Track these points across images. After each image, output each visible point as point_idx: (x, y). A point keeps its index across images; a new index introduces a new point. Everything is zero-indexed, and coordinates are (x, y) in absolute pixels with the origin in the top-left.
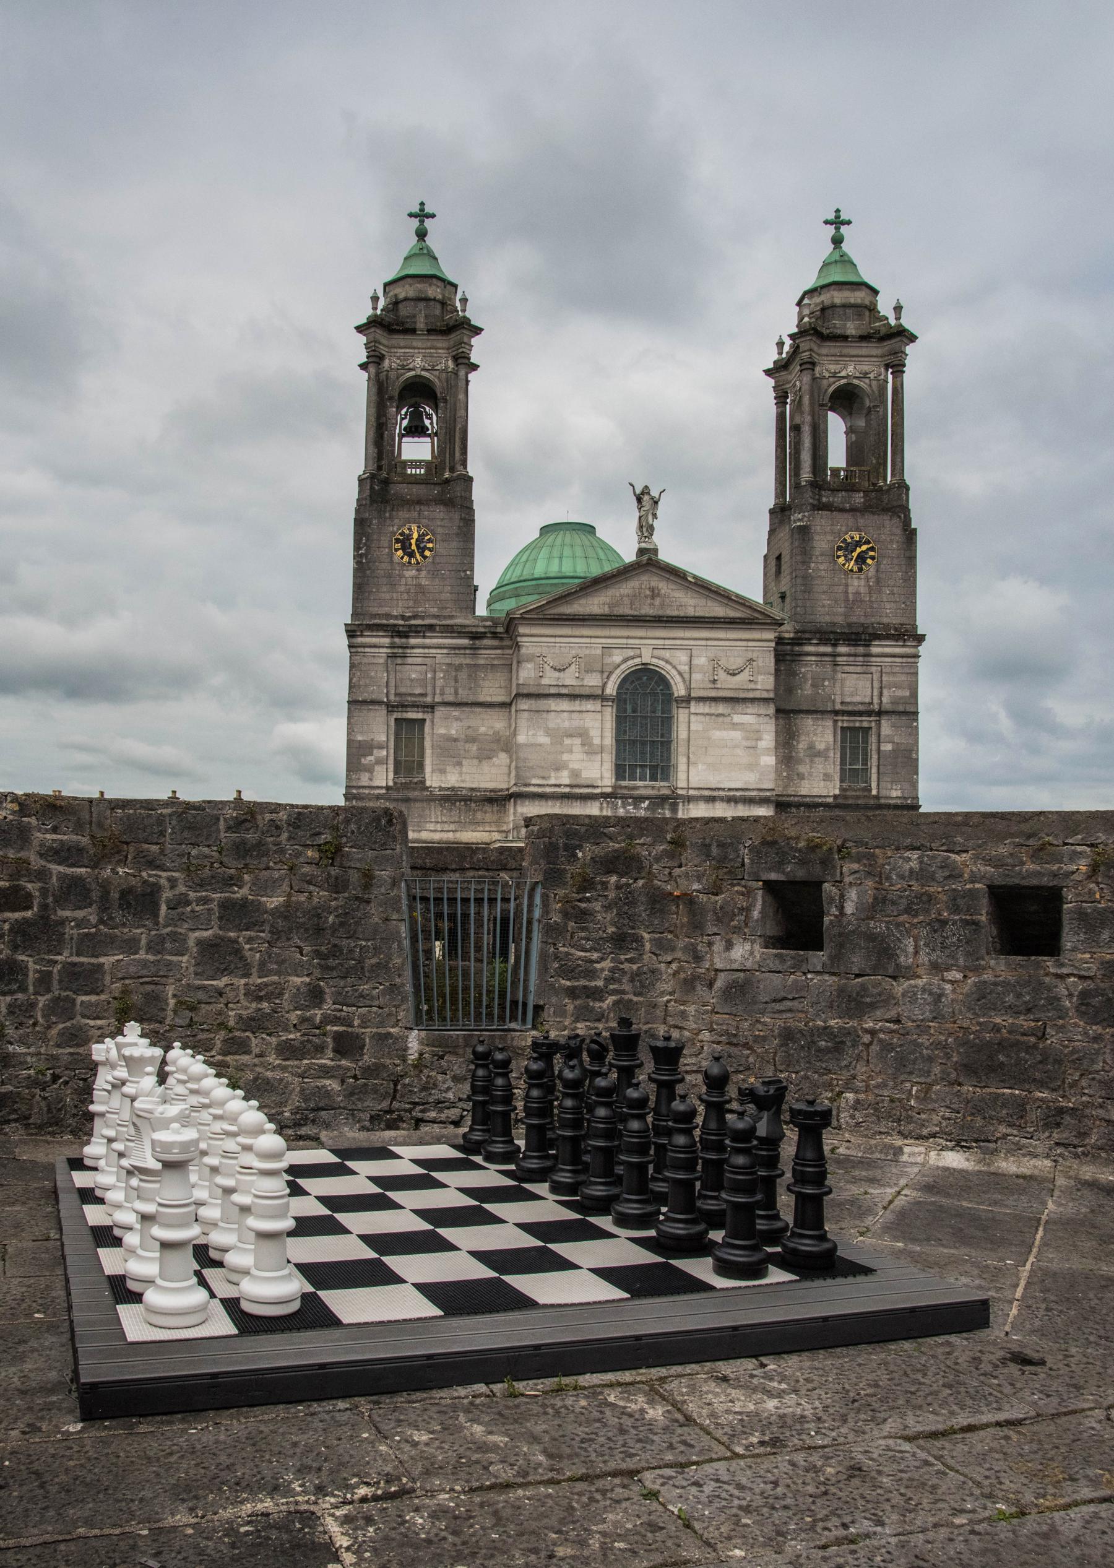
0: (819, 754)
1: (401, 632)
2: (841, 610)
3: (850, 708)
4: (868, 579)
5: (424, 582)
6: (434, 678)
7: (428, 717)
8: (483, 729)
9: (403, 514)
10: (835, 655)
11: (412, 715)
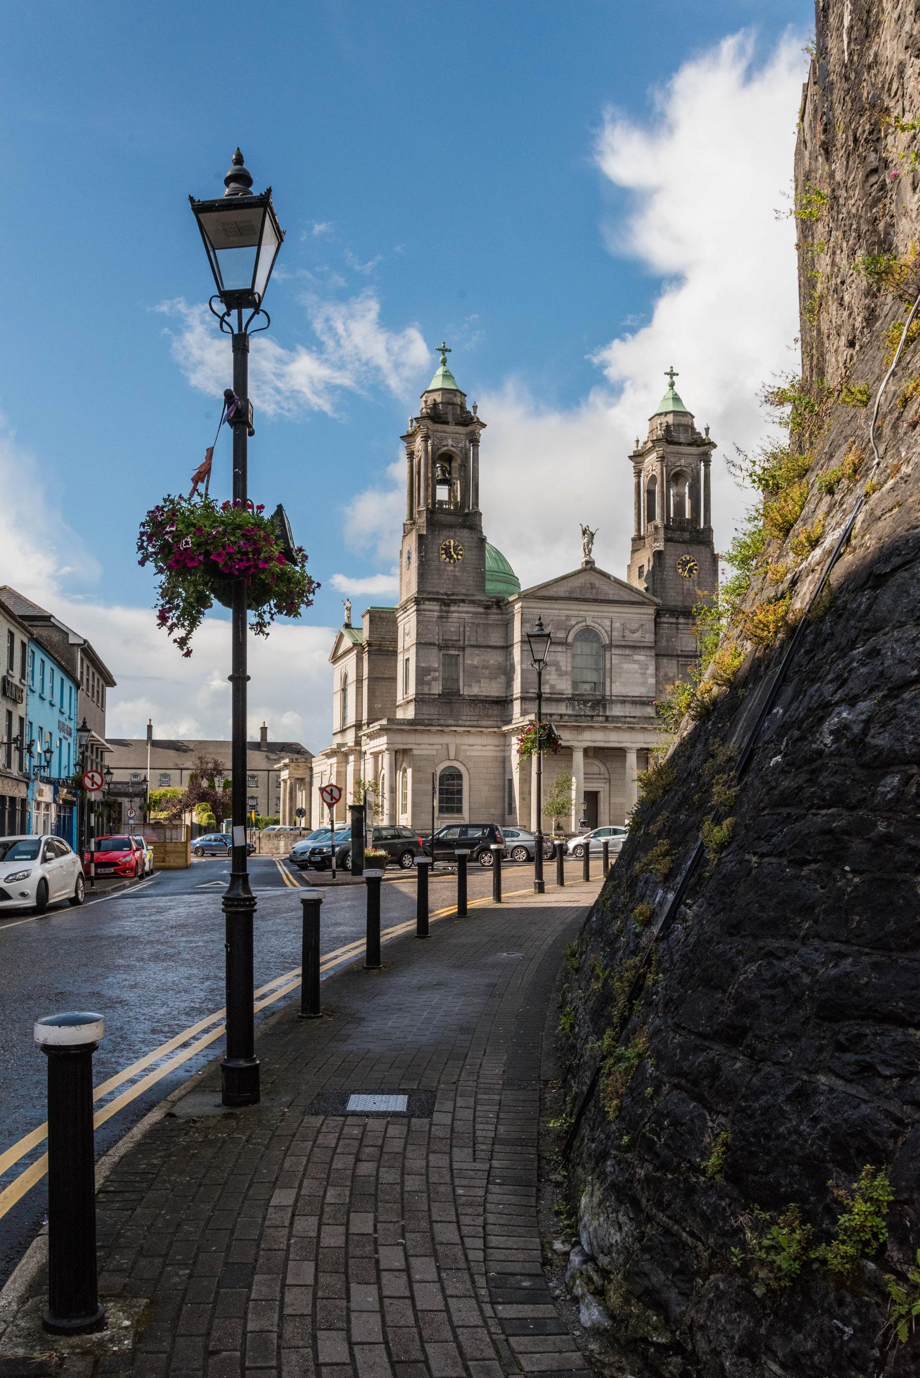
0: (669, 679)
1: (446, 602)
2: (681, 599)
3: (685, 654)
4: (694, 582)
5: (457, 574)
6: (464, 631)
7: (461, 653)
8: (492, 662)
9: (445, 533)
10: (677, 624)
11: (452, 652)
